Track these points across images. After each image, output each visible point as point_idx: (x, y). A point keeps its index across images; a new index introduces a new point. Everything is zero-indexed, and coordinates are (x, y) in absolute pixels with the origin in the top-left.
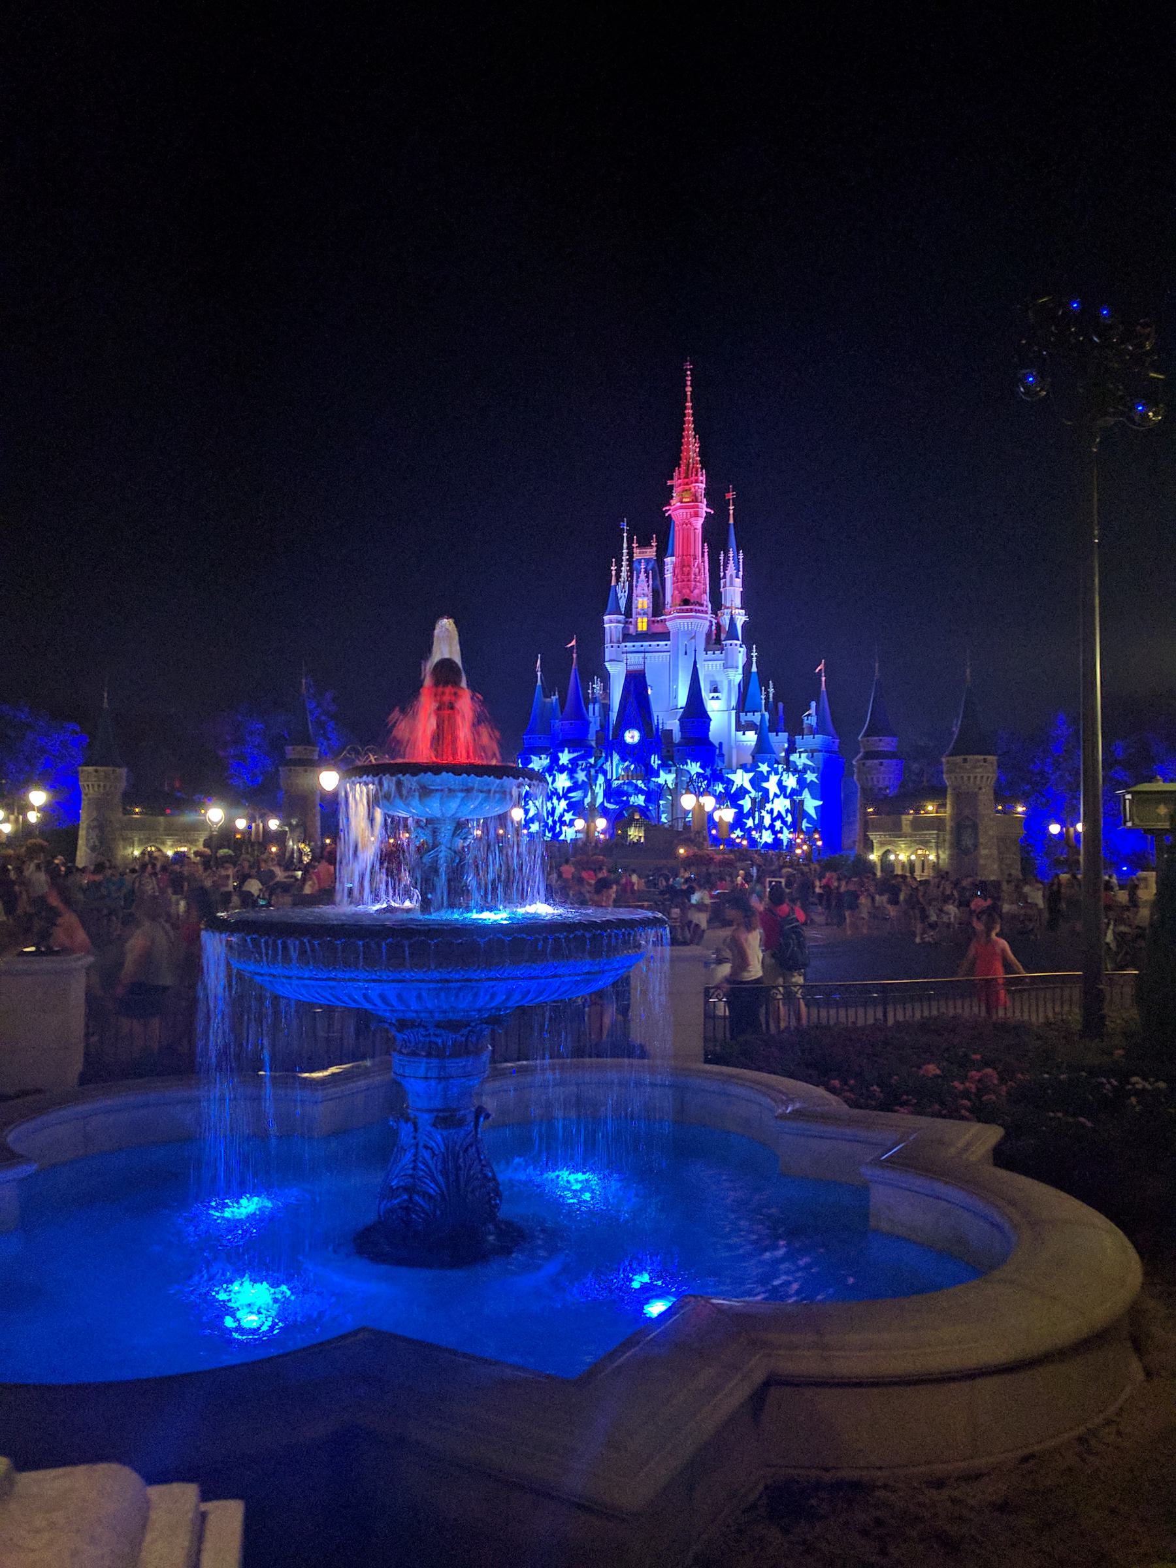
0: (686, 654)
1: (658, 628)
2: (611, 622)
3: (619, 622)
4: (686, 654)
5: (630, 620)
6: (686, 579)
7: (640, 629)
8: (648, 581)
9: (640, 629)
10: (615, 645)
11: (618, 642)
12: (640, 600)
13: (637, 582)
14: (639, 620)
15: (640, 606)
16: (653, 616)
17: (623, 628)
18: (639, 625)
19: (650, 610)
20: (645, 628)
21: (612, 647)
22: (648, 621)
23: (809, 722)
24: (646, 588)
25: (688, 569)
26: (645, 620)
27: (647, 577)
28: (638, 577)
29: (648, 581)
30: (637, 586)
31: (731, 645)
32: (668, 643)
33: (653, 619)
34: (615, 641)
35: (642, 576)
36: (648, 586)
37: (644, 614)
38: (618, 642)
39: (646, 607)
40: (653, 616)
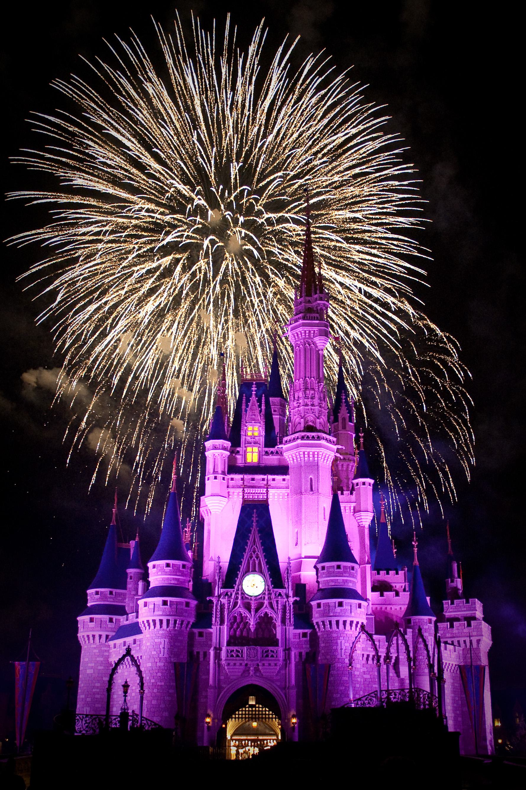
0: (312, 490)
1: (272, 460)
2: (215, 448)
3: (224, 449)
4: (312, 490)
5: (238, 449)
6: (309, 403)
7: (249, 460)
8: (260, 406)
9: (249, 460)
10: (220, 476)
11: (223, 473)
12: (250, 428)
13: (247, 406)
14: (249, 449)
15: (250, 434)
16: (265, 447)
17: (229, 457)
18: (249, 456)
19: (262, 440)
20: (255, 460)
21: (216, 478)
22: (259, 452)
23: (454, 585)
24: (257, 412)
25: (312, 392)
26: (256, 449)
27: (260, 401)
28: (248, 401)
29: (260, 406)
30: (246, 411)
31: (364, 484)
32: (287, 477)
33: (267, 449)
34: (220, 472)
35: (253, 398)
36: (261, 411)
37: (255, 443)
38: (223, 473)
39: (256, 434)
40: (266, 446)
